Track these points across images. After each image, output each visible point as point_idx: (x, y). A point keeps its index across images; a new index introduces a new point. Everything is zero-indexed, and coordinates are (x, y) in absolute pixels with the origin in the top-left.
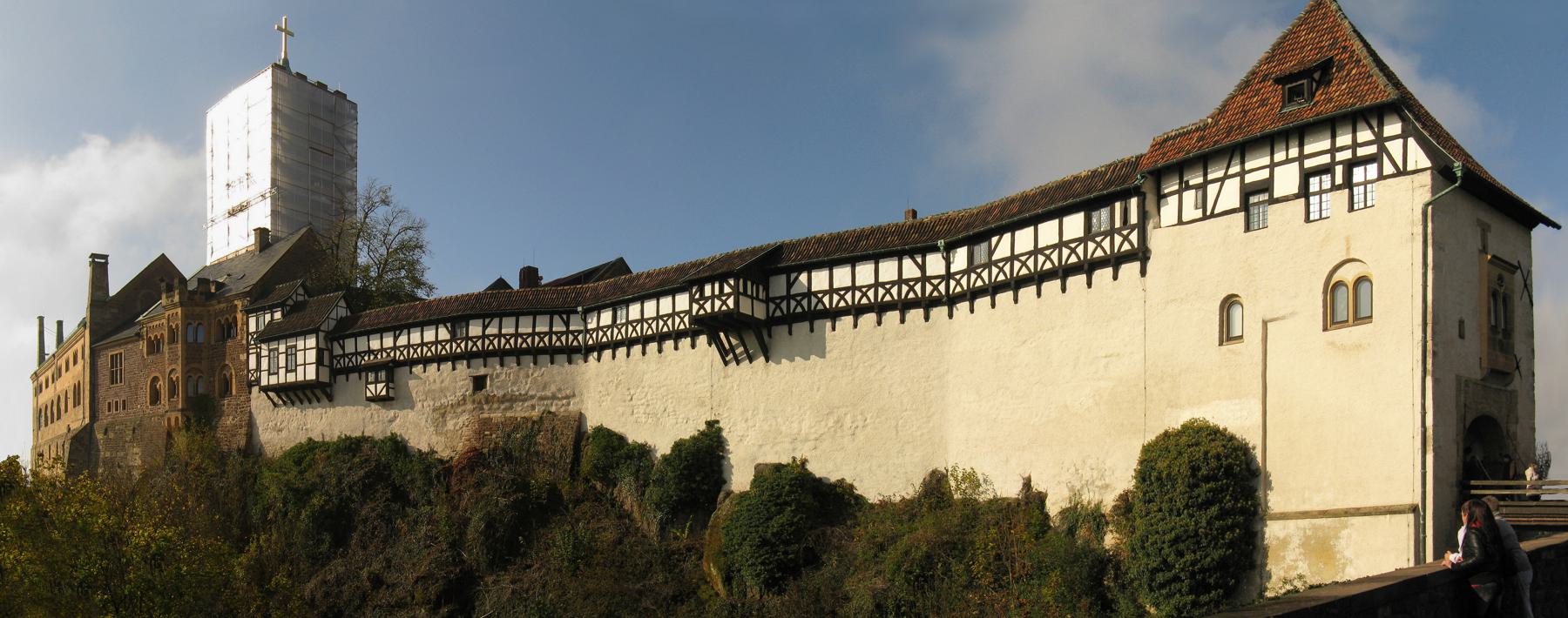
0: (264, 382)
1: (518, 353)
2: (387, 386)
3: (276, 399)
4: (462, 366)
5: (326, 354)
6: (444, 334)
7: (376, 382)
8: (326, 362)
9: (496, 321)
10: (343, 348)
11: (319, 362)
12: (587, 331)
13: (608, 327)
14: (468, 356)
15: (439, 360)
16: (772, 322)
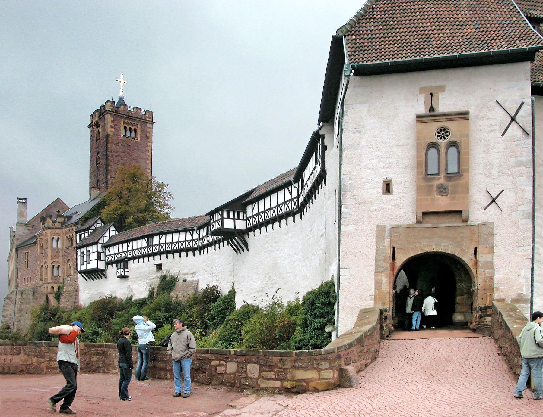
0: (79, 270)
1: (173, 252)
2: (124, 270)
3: (87, 278)
4: (151, 258)
5: (103, 255)
6: (145, 244)
7: (121, 268)
8: (103, 258)
9: (164, 236)
10: (109, 251)
11: (99, 258)
12: (200, 239)
13: (205, 236)
14: (154, 254)
15: (143, 256)
16: (249, 230)
